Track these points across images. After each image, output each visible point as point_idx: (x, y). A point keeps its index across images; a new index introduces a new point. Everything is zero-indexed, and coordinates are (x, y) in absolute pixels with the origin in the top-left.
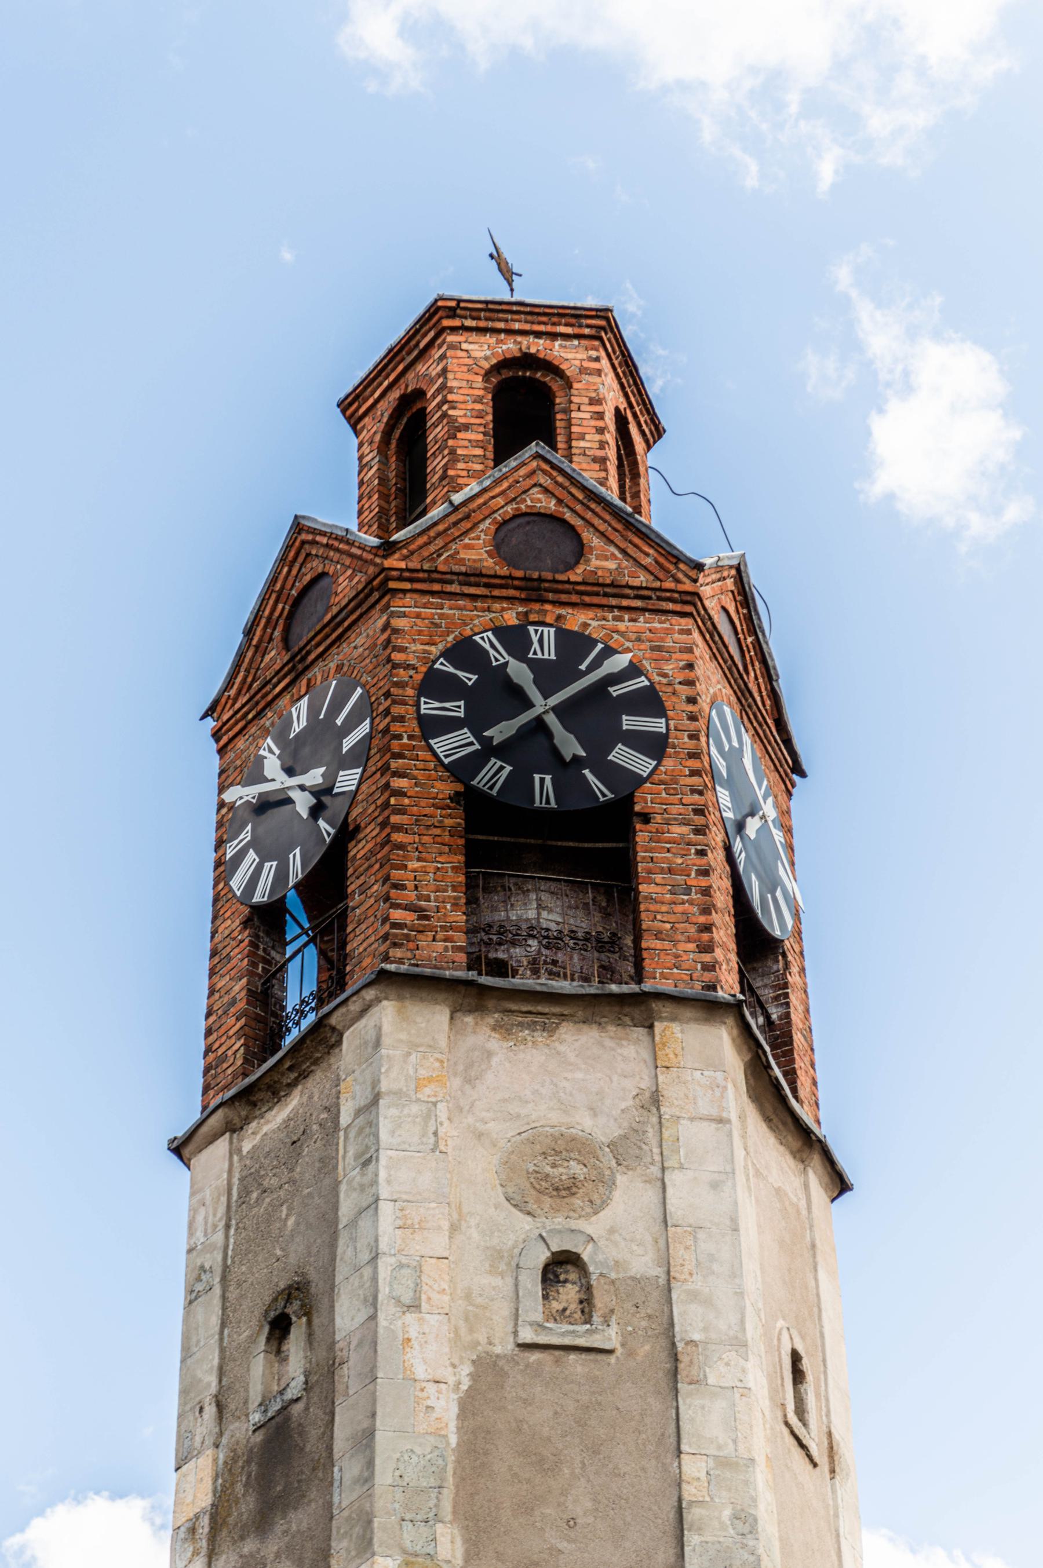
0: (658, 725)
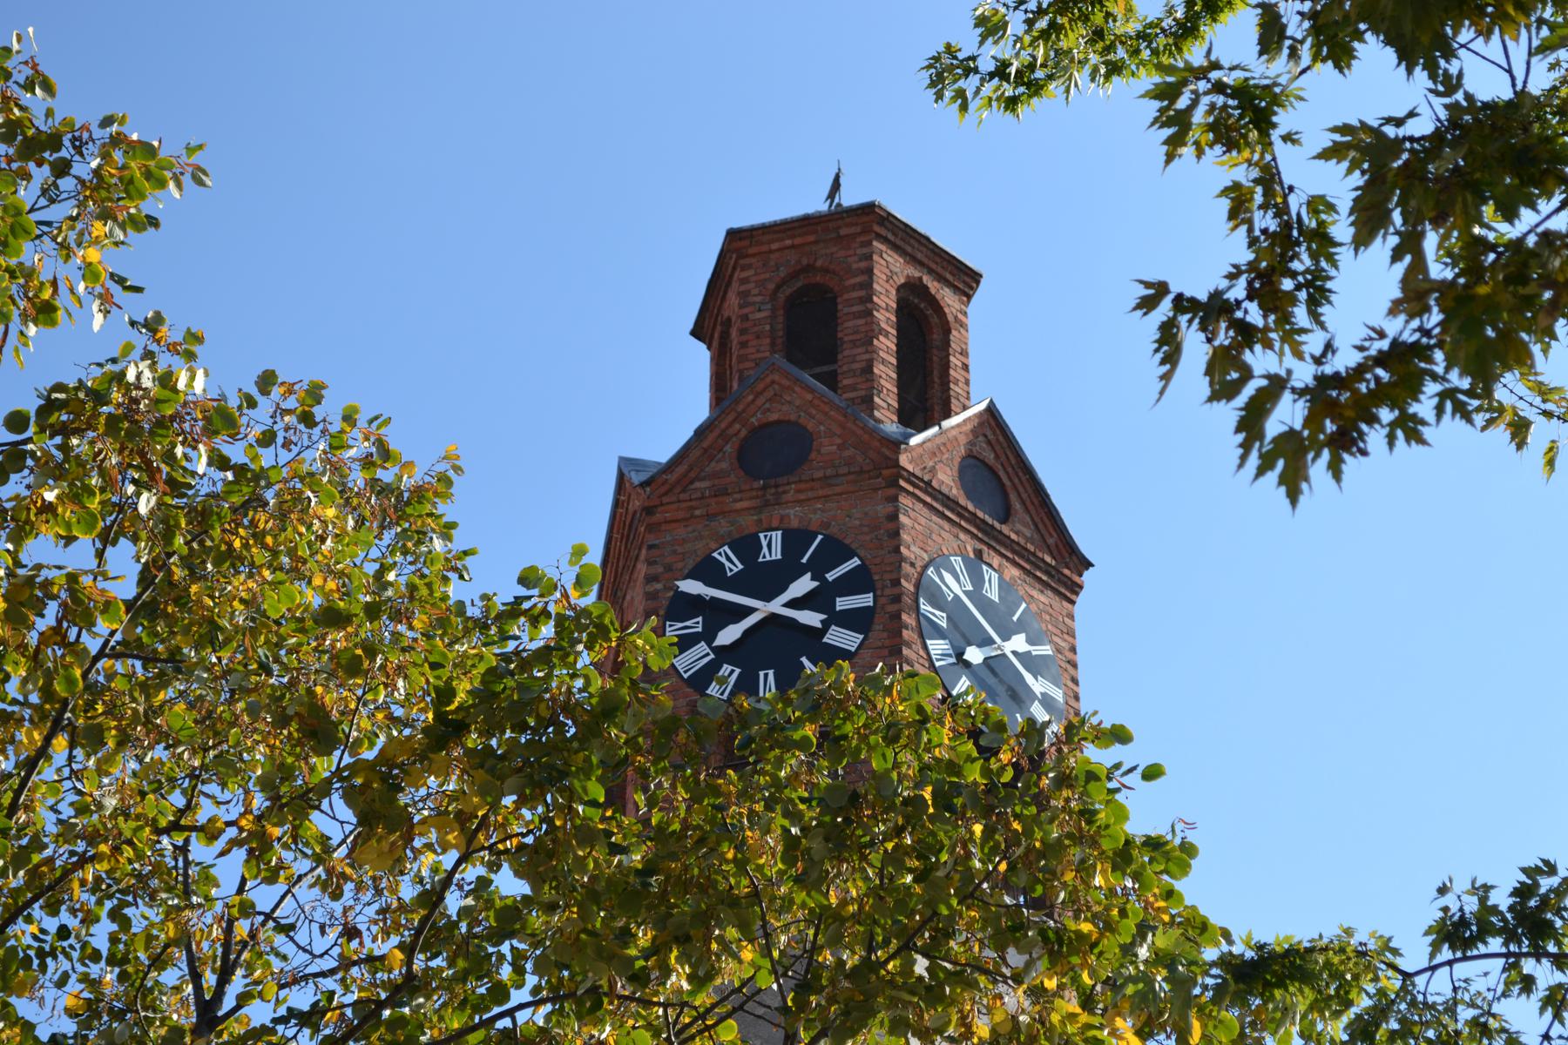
0: (866, 600)
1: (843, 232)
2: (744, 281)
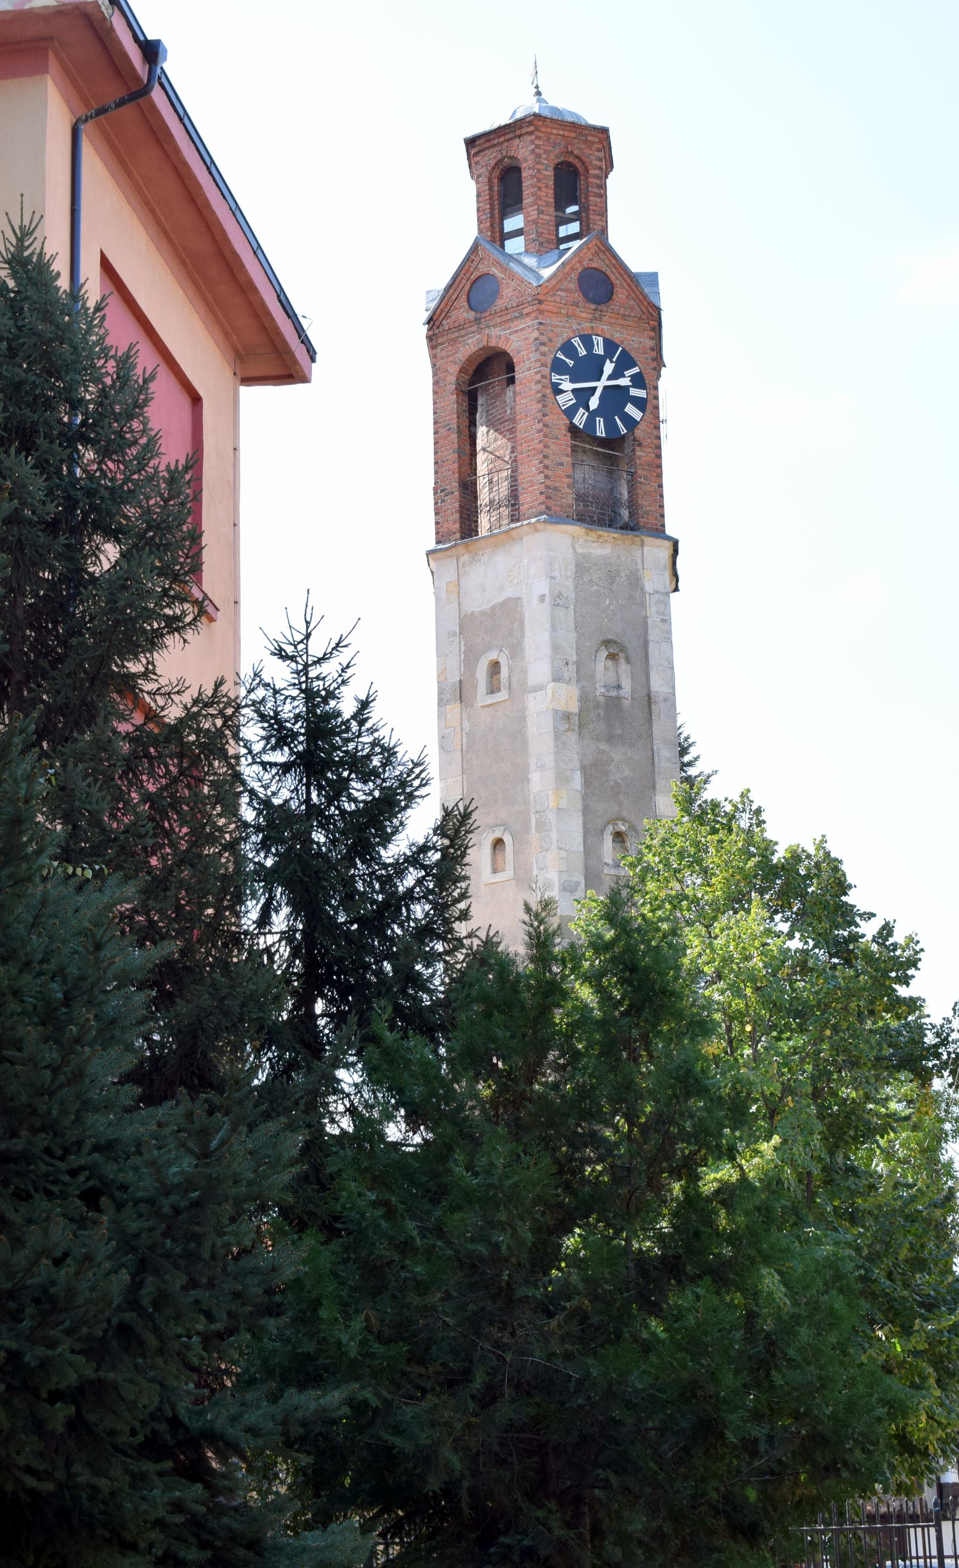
1: (590, 138)
2: (537, 146)
